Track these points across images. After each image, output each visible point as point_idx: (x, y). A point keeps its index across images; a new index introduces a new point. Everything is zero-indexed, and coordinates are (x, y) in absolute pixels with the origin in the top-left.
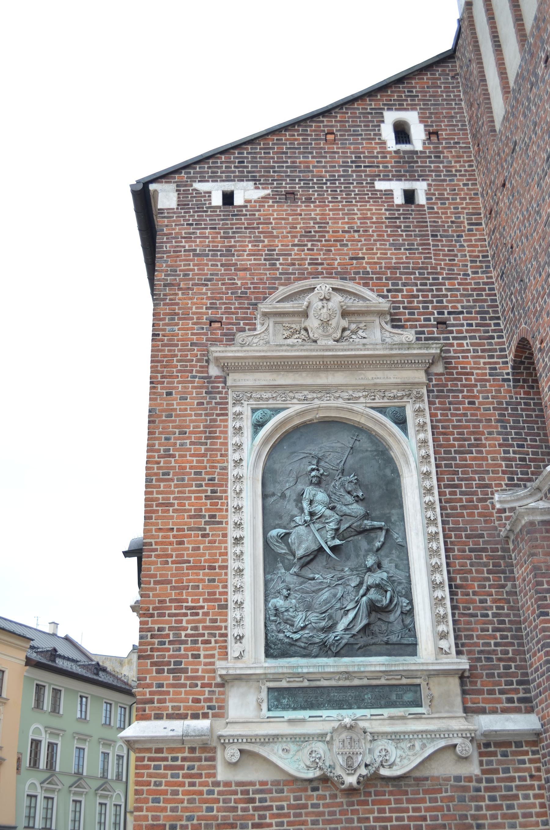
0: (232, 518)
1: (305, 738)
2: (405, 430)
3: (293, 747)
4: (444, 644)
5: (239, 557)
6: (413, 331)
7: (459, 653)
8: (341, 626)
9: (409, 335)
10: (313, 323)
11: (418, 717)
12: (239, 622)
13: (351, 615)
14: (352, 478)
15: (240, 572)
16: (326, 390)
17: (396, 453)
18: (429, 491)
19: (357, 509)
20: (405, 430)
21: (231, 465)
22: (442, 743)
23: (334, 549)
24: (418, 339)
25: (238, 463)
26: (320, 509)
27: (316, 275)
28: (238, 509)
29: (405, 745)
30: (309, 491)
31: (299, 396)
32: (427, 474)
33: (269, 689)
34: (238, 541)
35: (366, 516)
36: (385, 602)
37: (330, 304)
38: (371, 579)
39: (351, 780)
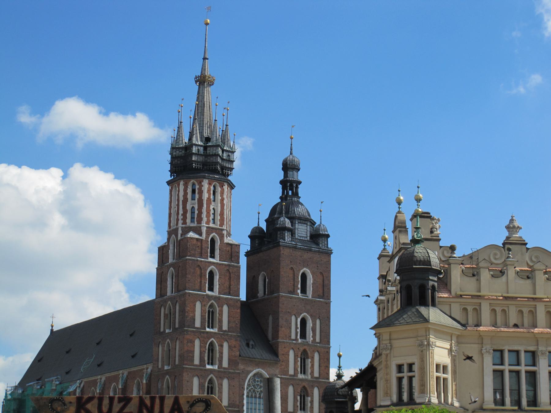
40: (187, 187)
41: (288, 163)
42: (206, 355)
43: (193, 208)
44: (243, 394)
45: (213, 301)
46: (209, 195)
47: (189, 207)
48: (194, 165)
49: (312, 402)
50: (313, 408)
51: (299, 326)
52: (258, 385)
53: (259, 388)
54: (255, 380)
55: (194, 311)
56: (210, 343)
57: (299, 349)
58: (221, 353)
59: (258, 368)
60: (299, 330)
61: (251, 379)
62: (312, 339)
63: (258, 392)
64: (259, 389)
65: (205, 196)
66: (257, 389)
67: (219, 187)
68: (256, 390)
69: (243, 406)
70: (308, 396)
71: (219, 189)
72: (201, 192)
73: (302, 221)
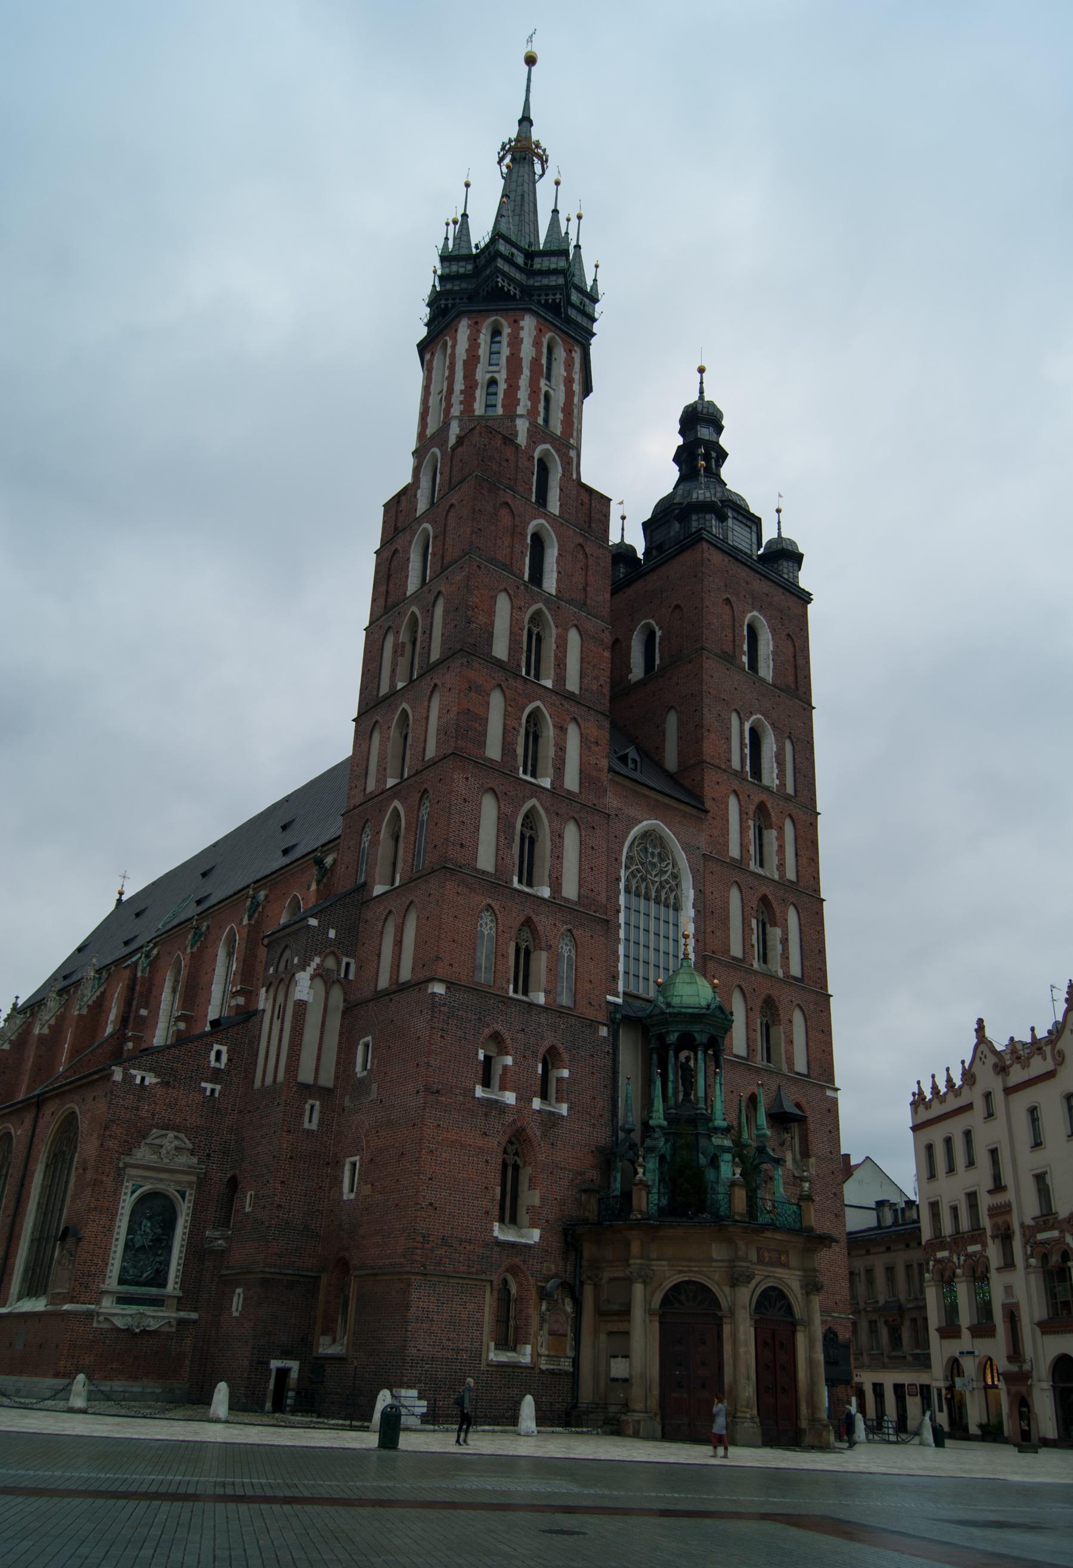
0: (116, 1230)
1: (126, 1315)
2: (184, 1201)
4: (176, 1286)
5: (116, 1246)
8: (145, 1275)
9: (195, 1160)
10: (163, 1151)
11: (162, 1311)
12: (111, 1271)
14: (161, 1218)
15: (115, 1252)
16: (161, 1180)
17: (178, 1209)
19: (159, 1231)
20: (184, 1201)
23: (149, 1246)
25: (123, 1208)
26: (148, 1230)
28: (119, 1227)
30: (145, 1222)
34: (117, 1240)
35: (163, 1234)
38: (158, 1259)
39: (137, 1330)
40: (479, 331)
41: (699, 409)
42: (521, 740)
43: (493, 382)
44: (618, 879)
45: (540, 605)
46: (539, 353)
47: (481, 375)
48: (499, 280)
49: (785, 941)
50: (788, 958)
51: (747, 741)
52: (654, 865)
53: (656, 875)
54: (646, 849)
55: (491, 613)
56: (529, 716)
57: (749, 796)
58: (561, 749)
59: (656, 819)
60: (747, 751)
61: (636, 844)
62: (777, 782)
63: (653, 883)
64: (656, 875)
65: (527, 351)
66: (651, 875)
67: (562, 350)
68: (649, 876)
69: (618, 911)
70: (774, 924)
71: (560, 354)
72: (515, 342)
73: (740, 518)
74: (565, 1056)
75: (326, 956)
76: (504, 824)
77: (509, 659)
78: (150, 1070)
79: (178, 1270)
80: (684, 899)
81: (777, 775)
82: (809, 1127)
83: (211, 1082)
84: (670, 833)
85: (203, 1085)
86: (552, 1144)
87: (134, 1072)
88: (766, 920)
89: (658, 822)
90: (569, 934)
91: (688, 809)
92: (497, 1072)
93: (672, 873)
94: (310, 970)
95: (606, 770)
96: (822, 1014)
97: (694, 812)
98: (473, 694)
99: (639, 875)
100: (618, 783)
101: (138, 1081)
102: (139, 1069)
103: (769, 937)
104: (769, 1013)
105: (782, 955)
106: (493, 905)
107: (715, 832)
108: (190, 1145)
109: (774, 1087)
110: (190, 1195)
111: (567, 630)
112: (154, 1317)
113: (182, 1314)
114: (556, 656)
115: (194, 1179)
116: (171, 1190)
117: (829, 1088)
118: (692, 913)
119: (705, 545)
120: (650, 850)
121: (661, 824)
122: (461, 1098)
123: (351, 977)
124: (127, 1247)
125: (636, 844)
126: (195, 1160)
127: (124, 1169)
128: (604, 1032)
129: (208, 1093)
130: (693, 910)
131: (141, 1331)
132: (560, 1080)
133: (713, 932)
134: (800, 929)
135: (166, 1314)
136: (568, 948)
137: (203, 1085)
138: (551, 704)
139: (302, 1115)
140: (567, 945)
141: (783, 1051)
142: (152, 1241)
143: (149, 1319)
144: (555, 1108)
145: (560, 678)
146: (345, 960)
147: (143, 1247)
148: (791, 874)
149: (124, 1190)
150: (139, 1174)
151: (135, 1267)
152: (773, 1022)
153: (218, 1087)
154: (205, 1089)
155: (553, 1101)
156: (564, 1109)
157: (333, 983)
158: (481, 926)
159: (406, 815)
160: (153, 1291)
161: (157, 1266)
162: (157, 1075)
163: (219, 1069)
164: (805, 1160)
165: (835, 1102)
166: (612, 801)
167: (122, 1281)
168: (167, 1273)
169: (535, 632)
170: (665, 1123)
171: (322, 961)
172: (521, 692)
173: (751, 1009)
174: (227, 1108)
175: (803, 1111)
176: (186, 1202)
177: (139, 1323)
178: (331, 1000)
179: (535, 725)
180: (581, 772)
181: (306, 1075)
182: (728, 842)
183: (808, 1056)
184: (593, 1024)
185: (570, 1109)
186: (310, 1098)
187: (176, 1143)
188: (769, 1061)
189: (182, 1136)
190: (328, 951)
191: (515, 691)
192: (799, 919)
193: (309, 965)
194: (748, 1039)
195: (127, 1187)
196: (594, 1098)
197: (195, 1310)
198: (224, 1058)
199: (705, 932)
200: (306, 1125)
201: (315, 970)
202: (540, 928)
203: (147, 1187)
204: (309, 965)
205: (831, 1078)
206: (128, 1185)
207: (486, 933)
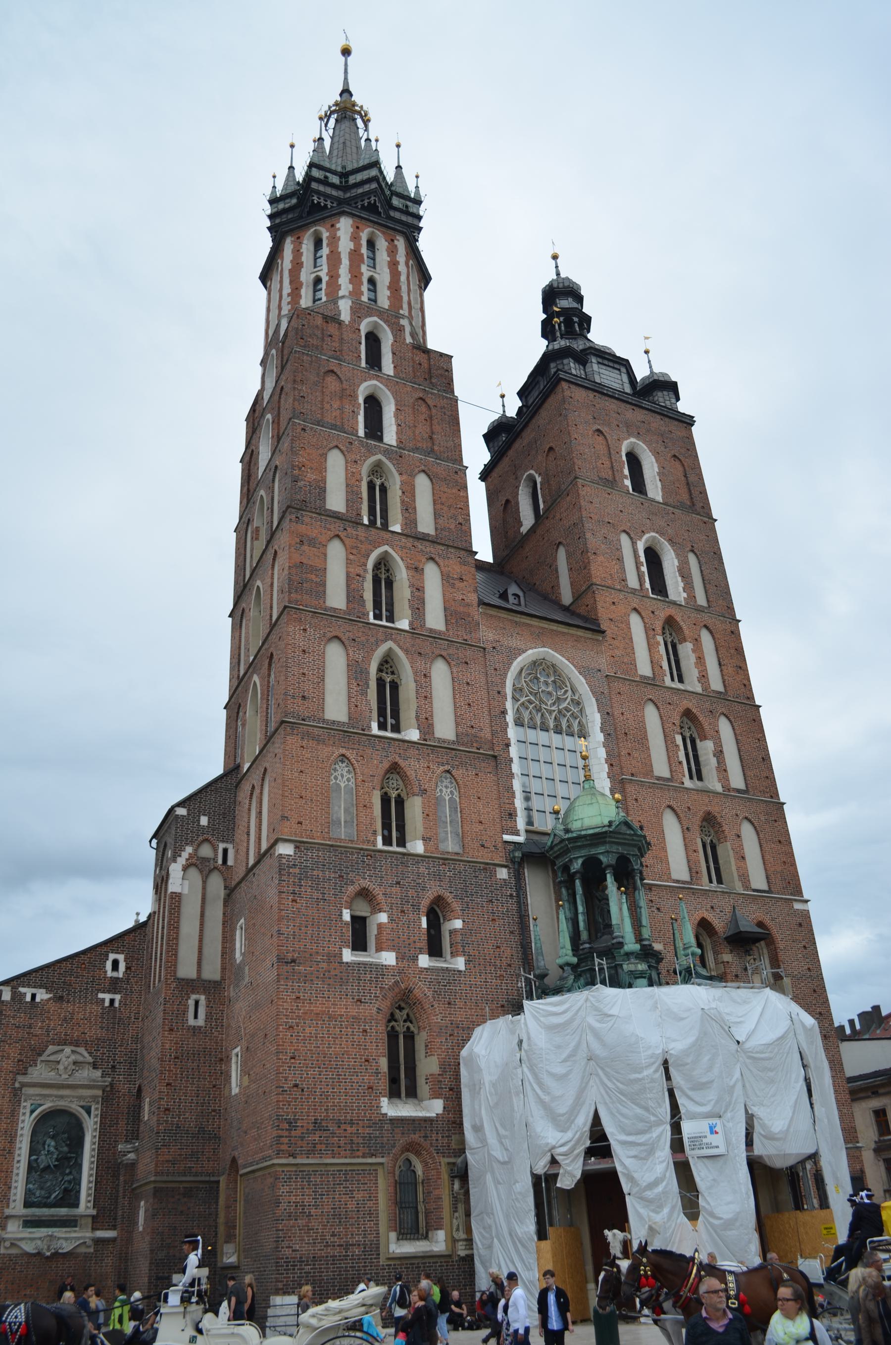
0: (17, 1152)
1: (34, 1239)
2: (90, 1116)
3: (29, 1242)
4: (89, 1205)
5: (18, 1168)
6: (101, 1071)
7: (94, 1207)
8: (53, 1197)
9: (98, 1073)
10: (61, 1067)
11: (75, 1231)
12: (15, 1194)
13: (57, 1193)
14: (66, 1135)
15: (17, 1174)
16: (62, 1097)
17: (84, 1125)
18: (94, 1144)
19: (66, 1149)
20: (90, 1116)
21: (19, 1129)
22: (82, 1241)
23: (55, 1166)
24: (103, 1074)
25: (22, 1128)
26: (52, 1149)
27: (65, 1044)
28: (20, 1148)
29: (69, 1242)
30: (48, 1141)
31: (51, 1099)
32: (95, 1137)
33: (24, 1221)
34: (19, 1162)
35: (69, 1152)
36: (71, 1188)
37: (70, 1060)
38: (67, 1178)
39: (48, 1254)
42: (368, 586)
44: (504, 712)
49: (719, 754)
50: (725, 770)
53: (554, 704)
55: (322, 469)
57: (653, 612)
58: (418, 590)
60: (644, 569)
63: (550, 712)
64: (554, 704)
66: (546, 704)
69: (508, 745)
70: (704, 738)
73: (606, 362)
74: (456, 906)
75: (199, 845)
76: (356, 672)
77: (347, 511)
78: (41, 987)
79: (90, 1188)
80: (589, 725)
81: (684, 589)
82: (777, 945)
83: (109, 992)
84: (563, 659)
85: (101, 996)
86: (449, 1004)
87: (22, 990)
88: (695, 735)
89: (546, 649)
90: (448, 775)
91: (580, 633)
92: (372, 932)
93: (572, 700)
94: (182, 861)
95: (476, 605)
96: (776, 824)
97: (589, 635)
98: (305, 548)
99: (531, 707)
100: (491, 616)
101: (28, 998)
102: (29, 986)
103: (700, 752)
104: (712, 831)
105: (718, 768)
106: (348, 754)
107: (618, 653)
108: (90, 1059)
109: (728, 909)
110: (96, 1109)
111: (413, 476)
112: (66, 1239)
113: (101, 1234)
114: (403, 502)
115: (99, 1093)
116: (75, 1107)
117: (796, 900)
118: (601, 737)
119: (564, 385)
120: (542, 679)
121: (550, 651)
122: (324, 965)
123: (230, 862)
124: (31, 1168)
125: (523, 675)
126: (98, 1073)
127: (20, 1089)
128: (503, 874)
129: (107, 1004)
130: (602, 735)
131: (53, 1254)
132: (452, 932)
133: (629, 754)
134: (737, 739)
135: (79, 1235)
136: (449, 790)
137: (101, 996)
138: (402, 547)
139: (185, 1012)
140: (446, 787)
141: (734, 868)
142: (57, 1160)
143: (61, 1241)
144: (450, 963)
145: (410, 520)
146: (221, 846)
147: (48, 1167)
148: (716, 684)
149: (22, 1111)
150: (37, 1093)
151: (42, 1189)
152: (719, 840)
153: (118, 997)
154: (103, 1000)
155: (449, 956)
156: (460, 963)
157: (211, 871)
158: (336, 778)
159: (261, 685)
160: (63, 1211)
161: (66, 1185)
162: (48, 990)
163: (118, 978)
164: (779, 982)
165: (806, 915)
166: (487, 634)
167: (27, 1205)
168: (79, 1192)
169: (378, 483)
170: (575, 960)
171: (196, 850)
172: (363, 539)
173: (688, 829)
174: (129, 1018)
175: (768, 930)
176: (92, 1116)
177: (49, 1246)
178: (209, 889)
179: (388, 571)
180: (445, 609)
181: (187, 969)
182: (635, 660)
183: (766, 870)
184: (489, 868)
185: (467, 963)
186: (193, 993)
187: (73, 1057)
188: (720, 881)
189: (82, 1050)
190: (201, 838)
191: (357, 539)
192: (734, 729)
193: (180, 856)
194: (688, 861)
195: (25, 1107)
196: (498, 947)
197: (114, 1228)
198: (122, 966)
199: (619, 756)
200: (191, 1022)
201: (187, 860)
202: (411, 773)
203: (48, 1105)
204: (180, 856)
205: (798, 891)
206: (26, 1106)
207: (343, 785)
